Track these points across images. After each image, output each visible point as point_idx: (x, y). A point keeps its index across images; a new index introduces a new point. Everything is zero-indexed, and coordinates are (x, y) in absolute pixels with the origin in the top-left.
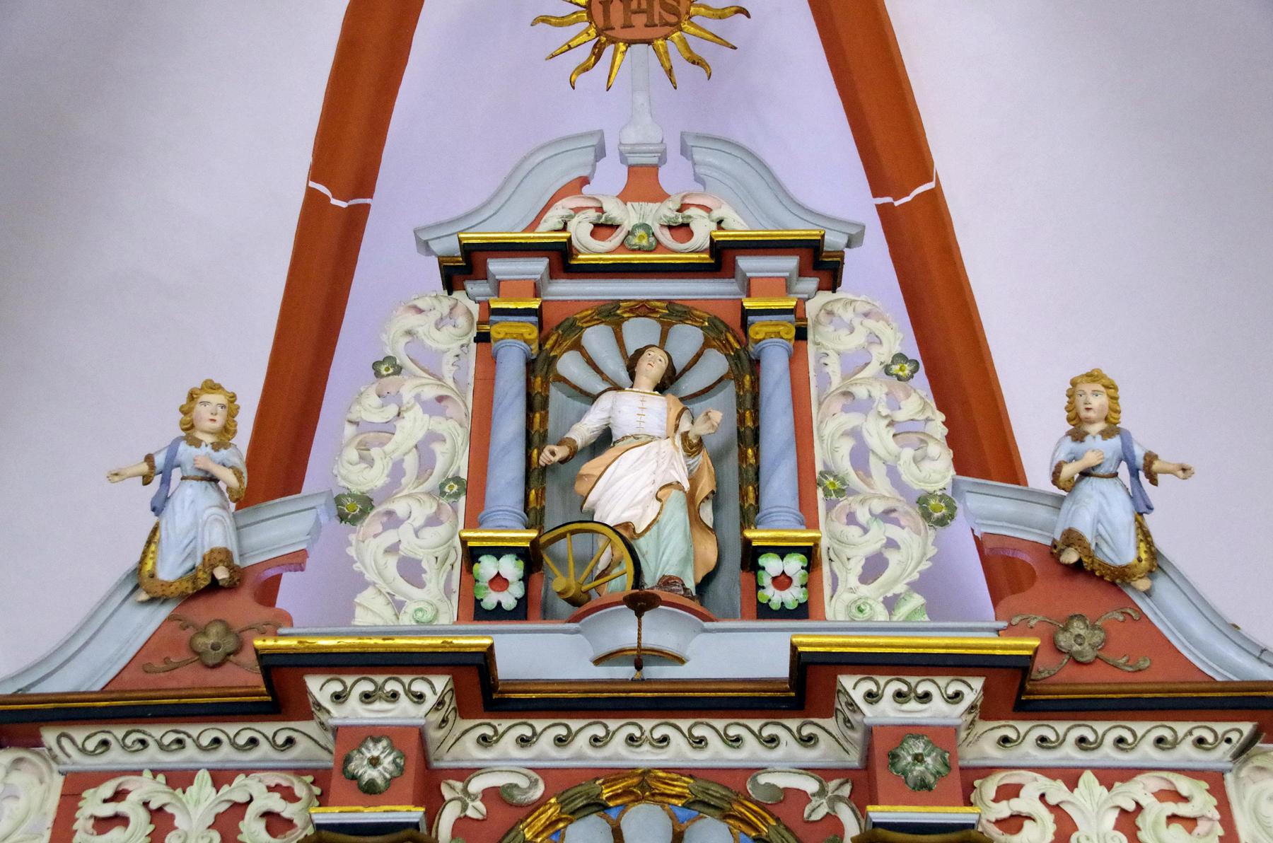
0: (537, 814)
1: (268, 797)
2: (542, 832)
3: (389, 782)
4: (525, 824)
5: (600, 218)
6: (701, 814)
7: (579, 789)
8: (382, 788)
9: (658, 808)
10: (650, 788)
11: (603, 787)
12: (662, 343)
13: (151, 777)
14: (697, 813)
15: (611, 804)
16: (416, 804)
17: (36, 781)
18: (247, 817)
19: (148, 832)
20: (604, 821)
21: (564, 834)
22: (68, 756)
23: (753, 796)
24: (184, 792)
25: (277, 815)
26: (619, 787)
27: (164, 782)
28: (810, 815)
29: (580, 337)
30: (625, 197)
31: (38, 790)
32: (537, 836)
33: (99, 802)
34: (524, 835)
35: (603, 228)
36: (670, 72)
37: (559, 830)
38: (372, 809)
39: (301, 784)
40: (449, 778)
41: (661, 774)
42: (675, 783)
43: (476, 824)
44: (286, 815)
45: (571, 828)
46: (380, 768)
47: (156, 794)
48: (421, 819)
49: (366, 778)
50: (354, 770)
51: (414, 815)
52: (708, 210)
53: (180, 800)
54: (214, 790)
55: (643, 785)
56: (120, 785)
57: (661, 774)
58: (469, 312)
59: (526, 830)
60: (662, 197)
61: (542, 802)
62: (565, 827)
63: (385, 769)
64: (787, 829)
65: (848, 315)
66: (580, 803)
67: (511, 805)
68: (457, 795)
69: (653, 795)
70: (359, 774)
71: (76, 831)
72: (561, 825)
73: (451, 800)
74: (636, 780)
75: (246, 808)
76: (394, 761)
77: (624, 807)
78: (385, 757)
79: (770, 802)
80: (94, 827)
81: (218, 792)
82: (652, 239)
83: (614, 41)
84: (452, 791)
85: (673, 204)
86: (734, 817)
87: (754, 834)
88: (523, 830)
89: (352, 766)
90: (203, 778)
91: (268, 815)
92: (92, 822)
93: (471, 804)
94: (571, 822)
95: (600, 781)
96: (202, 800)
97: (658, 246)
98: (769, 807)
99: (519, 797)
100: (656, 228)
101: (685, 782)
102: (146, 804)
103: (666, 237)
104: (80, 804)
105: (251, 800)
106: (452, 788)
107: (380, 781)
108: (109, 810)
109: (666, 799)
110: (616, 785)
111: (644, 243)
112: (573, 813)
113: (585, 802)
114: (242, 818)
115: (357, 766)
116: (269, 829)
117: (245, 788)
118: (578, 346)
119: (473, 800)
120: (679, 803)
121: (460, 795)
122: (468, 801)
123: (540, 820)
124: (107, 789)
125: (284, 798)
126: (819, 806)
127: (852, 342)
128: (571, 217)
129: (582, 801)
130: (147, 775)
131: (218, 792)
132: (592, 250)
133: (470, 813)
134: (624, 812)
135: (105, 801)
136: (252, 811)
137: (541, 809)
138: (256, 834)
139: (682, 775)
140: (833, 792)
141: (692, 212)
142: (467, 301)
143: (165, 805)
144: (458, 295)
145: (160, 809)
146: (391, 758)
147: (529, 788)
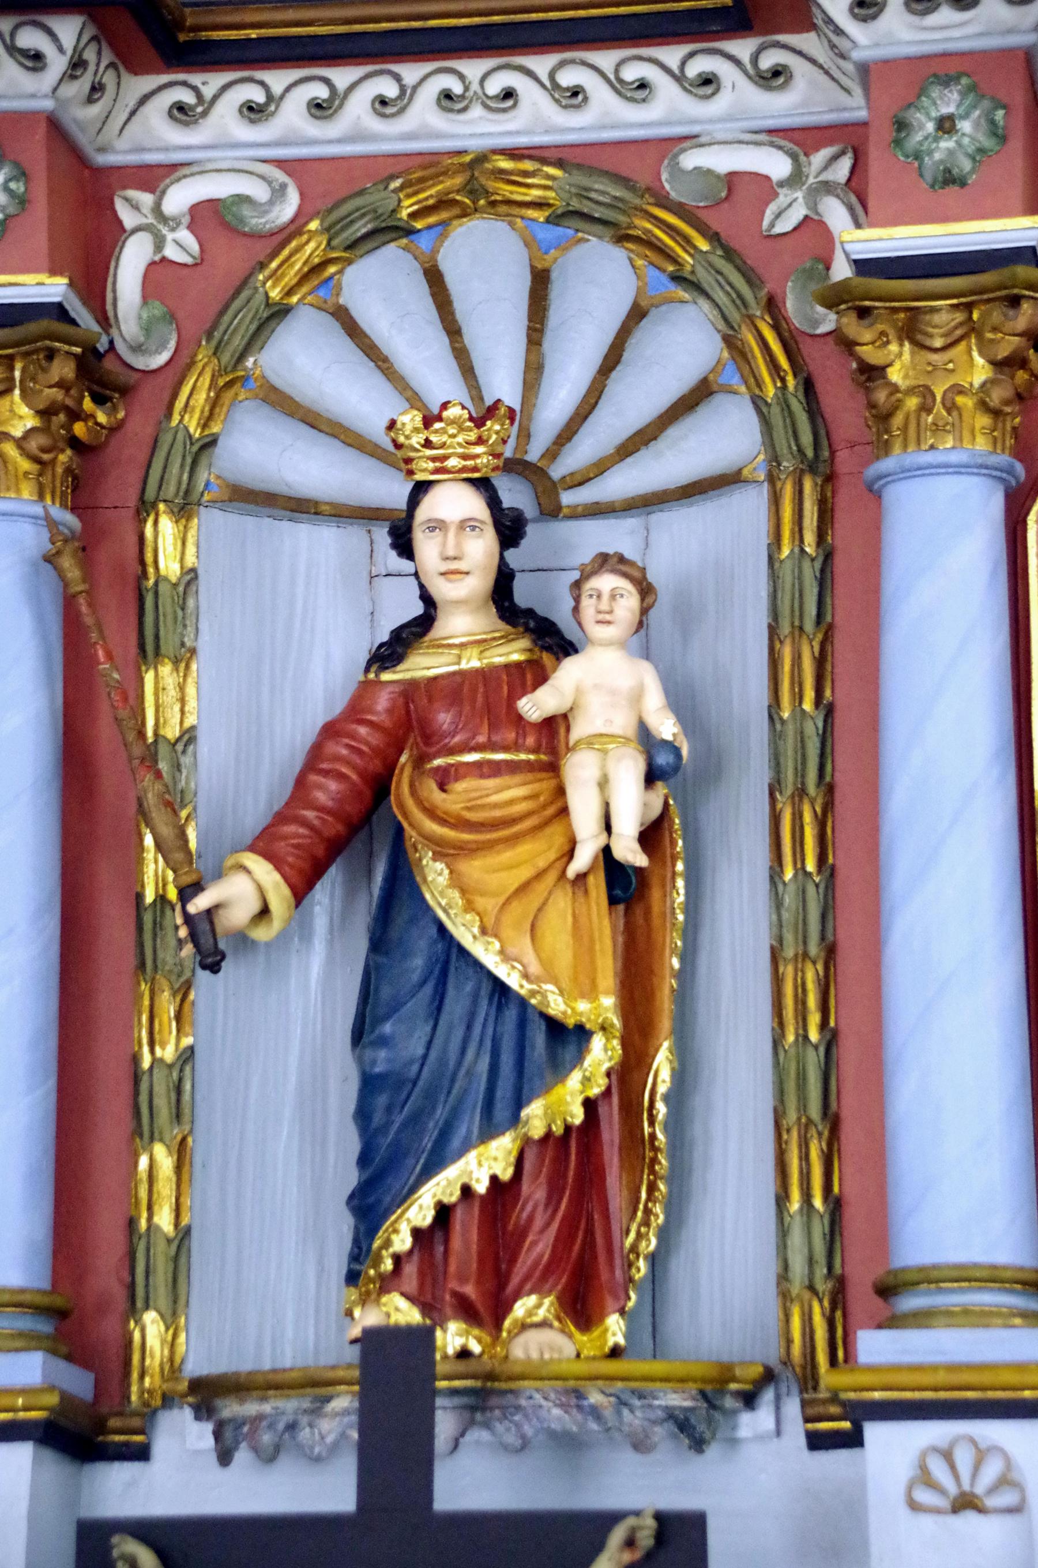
0: (286, 252)
2: (300, 283)
4: (267, 272)
6: (580, 235)
7: (358, 202)
9: (501, 226)
10: (487, 193)
11: (401, 196)
14: (571, 232)
15: (419, 225)
16: (53, 272)
20: (410, 257)
21: (339, 288)
23: (673, 195)
26: (430, 193)
28: (772, 225)
32: (290, 292)
34: (266, 294)
37: (331, 278)
40: (125, 187)
41: (505, 164)
42: (529, 181)
43: (185, 271)
45: (351, 272)
48: (64, 296)
51: (52, 290)
55: (473, 190)
57: (505, 164)
59: (269, 284)
61: (294, 229)
62: (341, 272)
64: (730, 254)
66: (362, 228)
68: (145, 221)
69: (493, 204)
72: (332, 269)
74: (458, 180)
77: (444, 224)
79: (702, 204)
84: (136, 212)
86: (637, 240)
87: (671, 268)
88: (264, 283)
93: (170, 236)
94: (350, 262)
95: (396, 184)
98: (701, 214)
99: (254, 221)
101: (549, 177)
106: (136, 207)
109: (516, 211)
110: (422, 190)
112: (351, 247)
113: (370, 227)
120: (540, 215)
121: (151, 220)
122: (165, 231)
123: (292, 265)
126: (790, 205)
129: (365, 225)
133: (171, 252)
134: (443, 236)
137: (294, 244)
139: (544, 161)
140: (816, 177)
147: (271, 202)
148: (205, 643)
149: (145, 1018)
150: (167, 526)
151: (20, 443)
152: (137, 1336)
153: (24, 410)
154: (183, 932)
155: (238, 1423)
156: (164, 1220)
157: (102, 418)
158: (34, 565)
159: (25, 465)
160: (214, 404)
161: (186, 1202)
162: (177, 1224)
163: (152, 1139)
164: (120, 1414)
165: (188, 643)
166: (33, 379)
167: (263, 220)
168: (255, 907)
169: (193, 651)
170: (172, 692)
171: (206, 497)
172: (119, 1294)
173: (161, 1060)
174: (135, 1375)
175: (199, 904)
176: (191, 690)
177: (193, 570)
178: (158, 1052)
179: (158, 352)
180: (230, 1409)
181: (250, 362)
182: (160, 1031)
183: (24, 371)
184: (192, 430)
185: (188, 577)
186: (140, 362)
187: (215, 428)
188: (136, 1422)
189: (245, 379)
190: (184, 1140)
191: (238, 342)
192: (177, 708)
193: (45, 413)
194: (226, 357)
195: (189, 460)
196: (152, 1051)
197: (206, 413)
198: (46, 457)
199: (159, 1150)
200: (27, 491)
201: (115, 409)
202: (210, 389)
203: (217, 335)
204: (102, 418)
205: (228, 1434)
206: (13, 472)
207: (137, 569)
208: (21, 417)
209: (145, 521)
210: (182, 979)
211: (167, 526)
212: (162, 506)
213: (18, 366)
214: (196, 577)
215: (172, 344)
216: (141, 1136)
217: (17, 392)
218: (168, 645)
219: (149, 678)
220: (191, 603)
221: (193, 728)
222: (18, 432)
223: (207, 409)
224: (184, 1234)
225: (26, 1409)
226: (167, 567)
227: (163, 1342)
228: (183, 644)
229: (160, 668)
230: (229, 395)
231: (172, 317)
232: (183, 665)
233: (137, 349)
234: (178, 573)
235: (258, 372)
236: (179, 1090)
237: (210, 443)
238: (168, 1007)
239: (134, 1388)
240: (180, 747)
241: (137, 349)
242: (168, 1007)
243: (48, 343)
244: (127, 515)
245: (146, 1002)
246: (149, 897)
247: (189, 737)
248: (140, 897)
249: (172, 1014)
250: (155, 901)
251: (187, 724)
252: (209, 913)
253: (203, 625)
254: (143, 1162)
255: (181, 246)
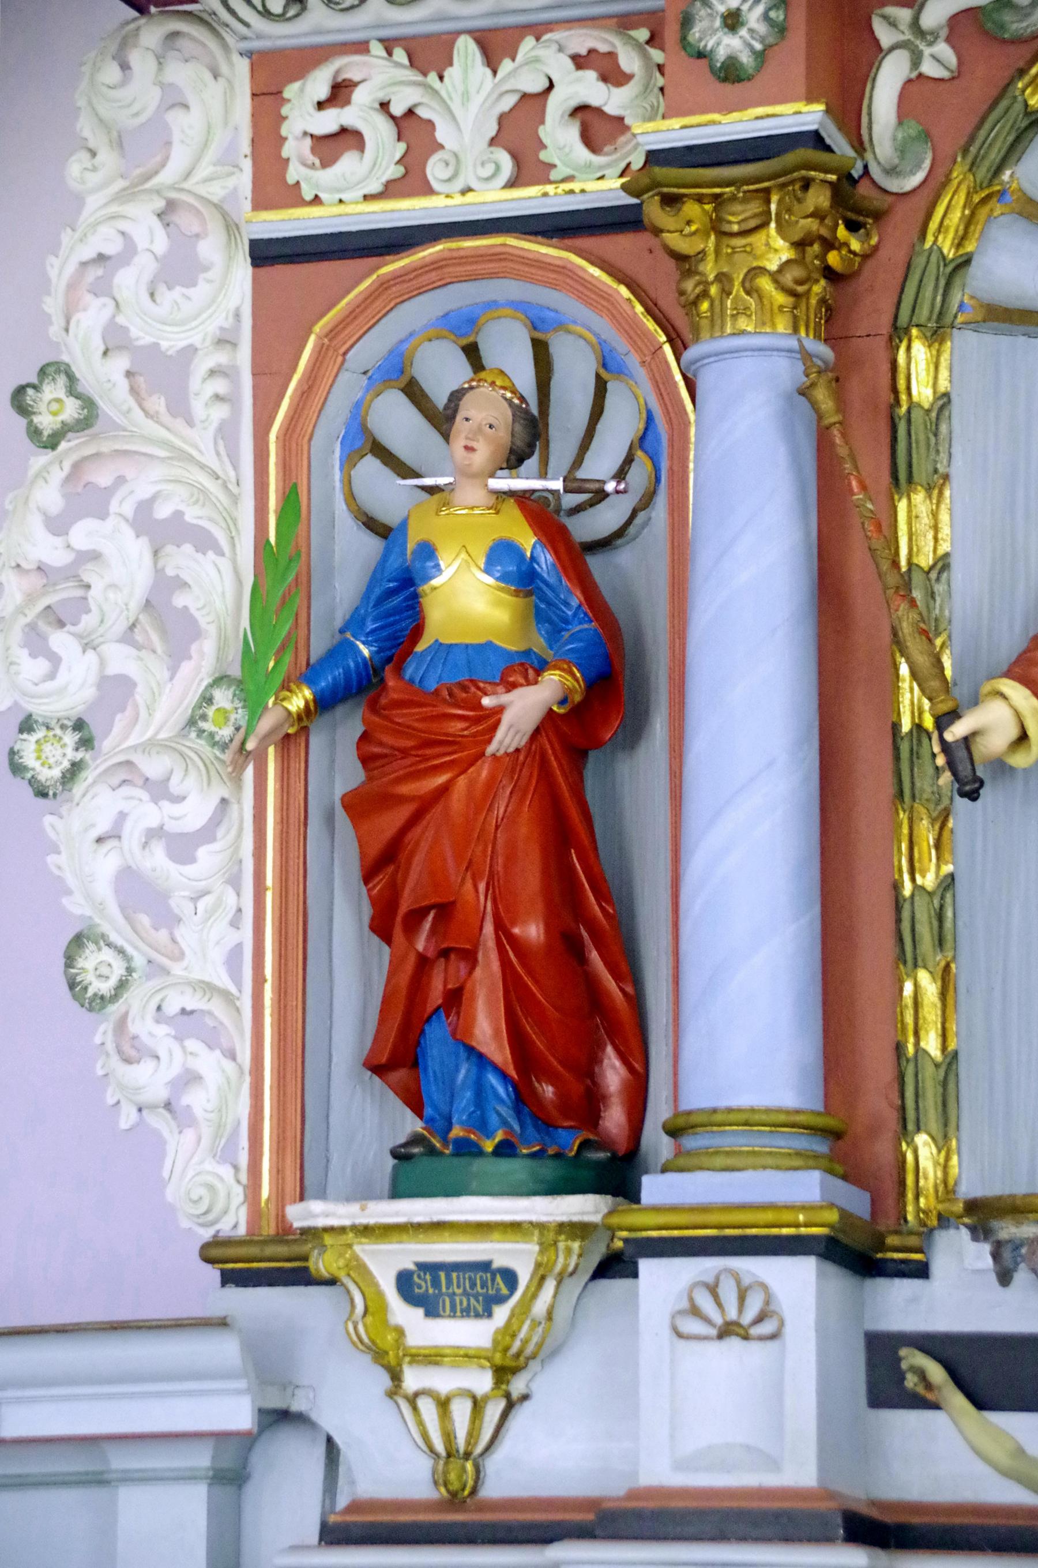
1: (578, 80)
3: (761, 57)
4: (1027, 79)
8: (751, 71)
13: (384, 54)
16: (810, 99)
17: (208, 76)
18: (548, 118)
19: (398, 156)
22: (247, 25)
24: (441, 78)
25: (598, 111)
27: (406, 62)
31: (214, 90)
33: (311, 108)
38: (735, 116)
39: (629, 48)
40: (883, 5)
43: (943, 86)
44: (611, 110)
46: (743, 32)
47: (396, 89)
48: (821, 124)
49: (721, 54)
50: (700, 40)
51: (809, 118)
53: (435, 92)
54: (488, 72)
56: (338, 72)
59: (1028, 91)
63: (751, 31)
67: (1004, 41)
68: (902, 38)
70: (709, 47)
71: (288, 160)
73: (892, 49)
75: (546, 100)
76: (765, 17)
78: (750, 9)
80: (313, 150)
81: (495, 72)
84: (893, 29)
88: (1023, 91)
89: (695, 34)
90: (466, 49)
91: (581, 111)
92: (308, 141)
93: (927, 51)
96: (472, 90)
99: (1014, 26)
102: (384, 106)
104: (284, 111)
105: (551, 86)
106: (893, 24)
107: (746, 59)
108: (329, 121)
114: (542, 122)
115: (704, 33)
116: (589, 140)
117: (538, 66)
119: (930, 44)
121: (908, 36)
122: (922, 46)
124: (319, 84)
125: (604, 78)
130: (377, 49)
131: (495, 72)
133: (929, 68)
135: (321, 105)
136: (557, 105)
138: (567, 150)
143: (416, 105)
145: (410, 112)
146: (760, 9)
148: (959, 468)
149: (904, 846)
150: (920, 351)
151: (775, 277)
152: (910, 1157)
153: (779, 243)
154: (941, 761)
155: (1016, 1245)
156: (931, 1044)
157: (855, 245)
158: (789, 398)
159: (781, 298)
160: (969, 222)
161: (952, 1027)
162: (944, 1048)
163: (916, 966)
164: (897, 1232)
165: (941, 469)
166: (789, 211)
167: (1024, 24)
168: (1013, 733)
169: (946, 477)
170: (926, 520)
171: (960, 319)
172: (892, 1117)
173: (922, 888)
174: (910, 1196)
175: (956, 732)
176: (944, 517)
177: (946, 395)
178: (919, 880)
179: (913, 173)
180: (1007, 1230)
181: (1006, 176)
182: (920, 858)
183: (780, 202)
184: (945, 251)
185: (941, 402)
186: (894, 185)
187: (970, 247)
188: (913, 1241)
189: (1002, 193)
190: (947, 966)
191: (994, 155)
192: (930, 535)
193: (800, 245)
194: (982, 172)
195: (942, 282)
196: (913, 879)
197: (961, 232)
198: (800, 289)
199: (923, 976)
200: (782, 325)
201: (868, 235)
202: (964, 207)
203: (973, 150)
204: (855, 245)
205: (1007, 1254)
206: (768, 307)
207: (888, 397)
208: (776, 250)
209: (898, 348)
210: (940, 807)
211: (920, 351)
212: (914, 332)
213: (775, 198)
214: (949, 401)
215: (927, 164)
216: (905, 963)
217: (773, 225)
218: (921, 472)
219: (902, 506)
220: (943, 428)
221: (947, 555)
222: (773, 266)
223: (962, 227)
224: (952, 1059)
225: (806, 1225)
226: (919, 393)
227: (936, 1163)
228: (936, 471)
229: (913, 496)
230: (983, 213)
231: (926, 135)
232: (936, 492)
233: (892, 171)
234: (931, 398)
235: (1014, 185)
236: (940, 917)
237: (966, 262)
238: (926, 833)
239: (910, 1208)
240: (933, 575)
241: (892, 171)
242: (926, 833)
243: (803, 173)
244: (881, 342)
245: (905, 831)
246: (906, 726)
247: (943, 564)
248: (896, 727)
249: (932, 842)
250: (911, 731)
251: (941, 551)
252: (967, 741)
253: (956, 450)
254: (908, 988)
255: (938, 61)
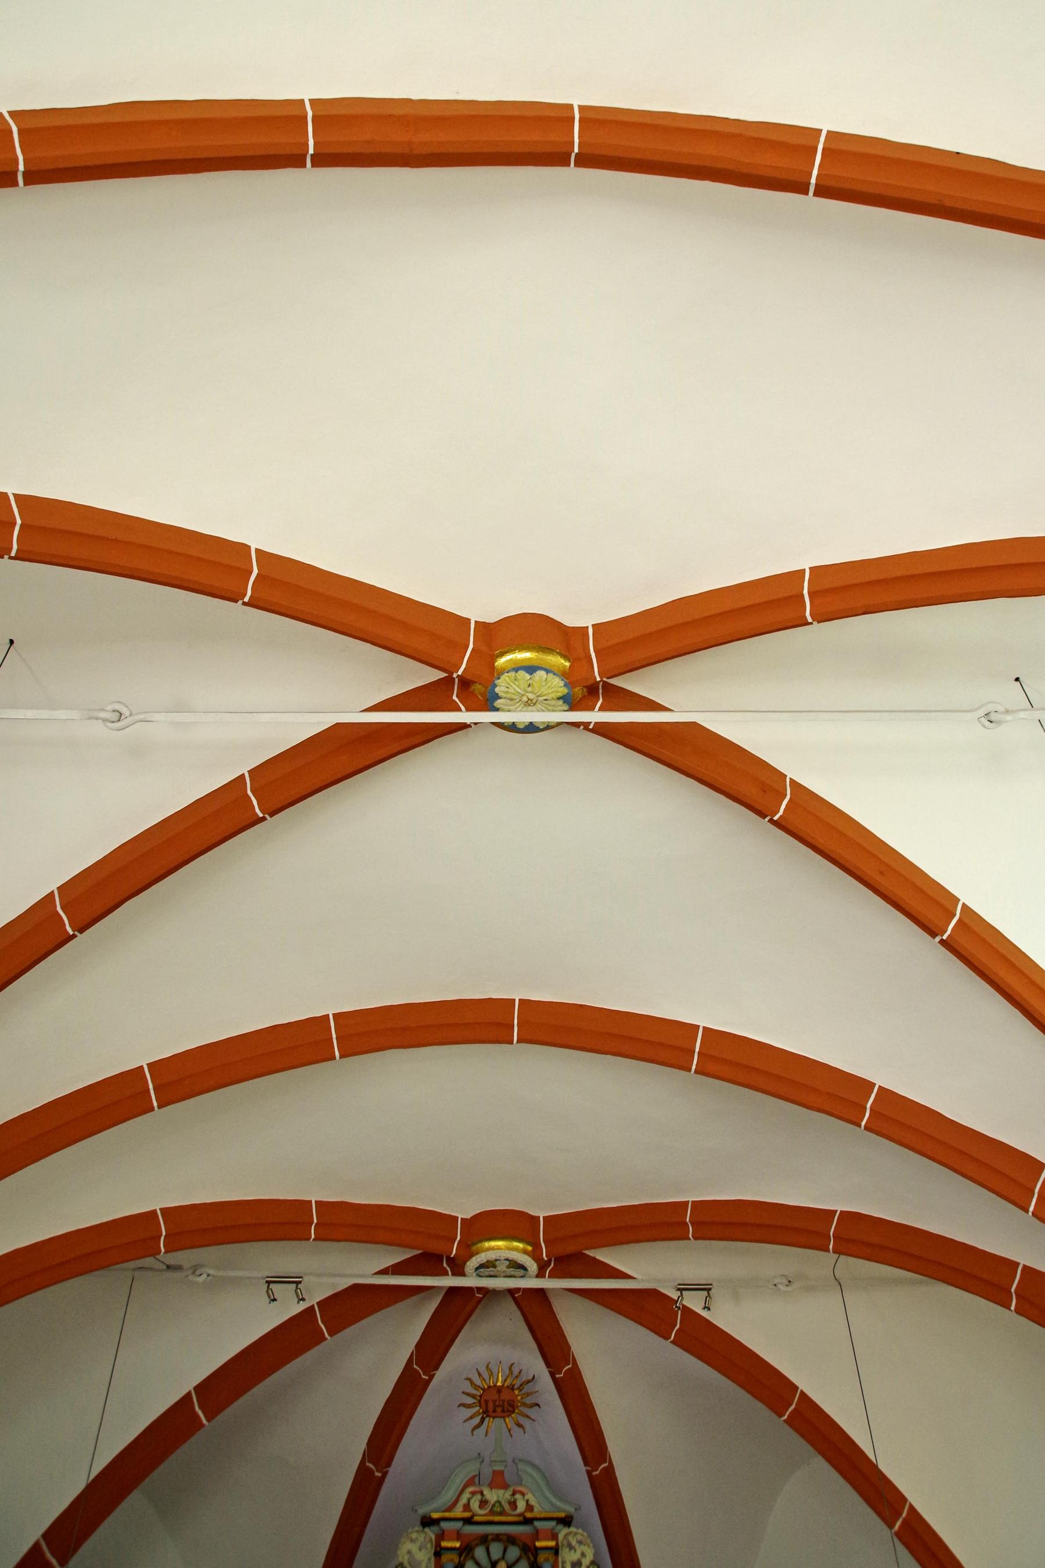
5: (482, 1499)
12: (503, 1558)
29: (473, 1553)
30: (492, 1486)
35: (483, 1503)
36: (509, 1431)
52: (523, 1494)
58: (431, 1540)
60: (505, 1487)
65: (574, 1543)
82: (502, 1509)
83: (487, 1416)
85: (510, 1492)
97: (503, 1513)
100: (503, 1503)
103: (507, 1507)
111: (499, 1510)
118: (473, 1558)
127: (574, 1556)
128: (472, 1498)
132: (481, 1514)
141: (518, 1496)
142: (431, 1533)
144: (427, 1530)
